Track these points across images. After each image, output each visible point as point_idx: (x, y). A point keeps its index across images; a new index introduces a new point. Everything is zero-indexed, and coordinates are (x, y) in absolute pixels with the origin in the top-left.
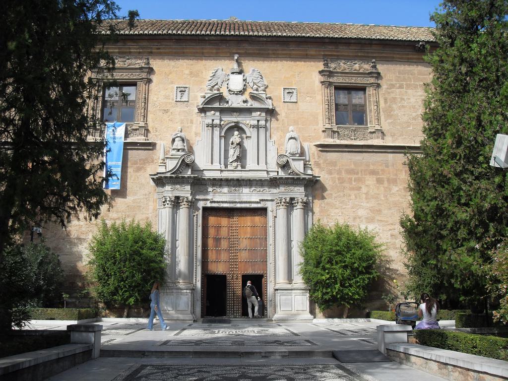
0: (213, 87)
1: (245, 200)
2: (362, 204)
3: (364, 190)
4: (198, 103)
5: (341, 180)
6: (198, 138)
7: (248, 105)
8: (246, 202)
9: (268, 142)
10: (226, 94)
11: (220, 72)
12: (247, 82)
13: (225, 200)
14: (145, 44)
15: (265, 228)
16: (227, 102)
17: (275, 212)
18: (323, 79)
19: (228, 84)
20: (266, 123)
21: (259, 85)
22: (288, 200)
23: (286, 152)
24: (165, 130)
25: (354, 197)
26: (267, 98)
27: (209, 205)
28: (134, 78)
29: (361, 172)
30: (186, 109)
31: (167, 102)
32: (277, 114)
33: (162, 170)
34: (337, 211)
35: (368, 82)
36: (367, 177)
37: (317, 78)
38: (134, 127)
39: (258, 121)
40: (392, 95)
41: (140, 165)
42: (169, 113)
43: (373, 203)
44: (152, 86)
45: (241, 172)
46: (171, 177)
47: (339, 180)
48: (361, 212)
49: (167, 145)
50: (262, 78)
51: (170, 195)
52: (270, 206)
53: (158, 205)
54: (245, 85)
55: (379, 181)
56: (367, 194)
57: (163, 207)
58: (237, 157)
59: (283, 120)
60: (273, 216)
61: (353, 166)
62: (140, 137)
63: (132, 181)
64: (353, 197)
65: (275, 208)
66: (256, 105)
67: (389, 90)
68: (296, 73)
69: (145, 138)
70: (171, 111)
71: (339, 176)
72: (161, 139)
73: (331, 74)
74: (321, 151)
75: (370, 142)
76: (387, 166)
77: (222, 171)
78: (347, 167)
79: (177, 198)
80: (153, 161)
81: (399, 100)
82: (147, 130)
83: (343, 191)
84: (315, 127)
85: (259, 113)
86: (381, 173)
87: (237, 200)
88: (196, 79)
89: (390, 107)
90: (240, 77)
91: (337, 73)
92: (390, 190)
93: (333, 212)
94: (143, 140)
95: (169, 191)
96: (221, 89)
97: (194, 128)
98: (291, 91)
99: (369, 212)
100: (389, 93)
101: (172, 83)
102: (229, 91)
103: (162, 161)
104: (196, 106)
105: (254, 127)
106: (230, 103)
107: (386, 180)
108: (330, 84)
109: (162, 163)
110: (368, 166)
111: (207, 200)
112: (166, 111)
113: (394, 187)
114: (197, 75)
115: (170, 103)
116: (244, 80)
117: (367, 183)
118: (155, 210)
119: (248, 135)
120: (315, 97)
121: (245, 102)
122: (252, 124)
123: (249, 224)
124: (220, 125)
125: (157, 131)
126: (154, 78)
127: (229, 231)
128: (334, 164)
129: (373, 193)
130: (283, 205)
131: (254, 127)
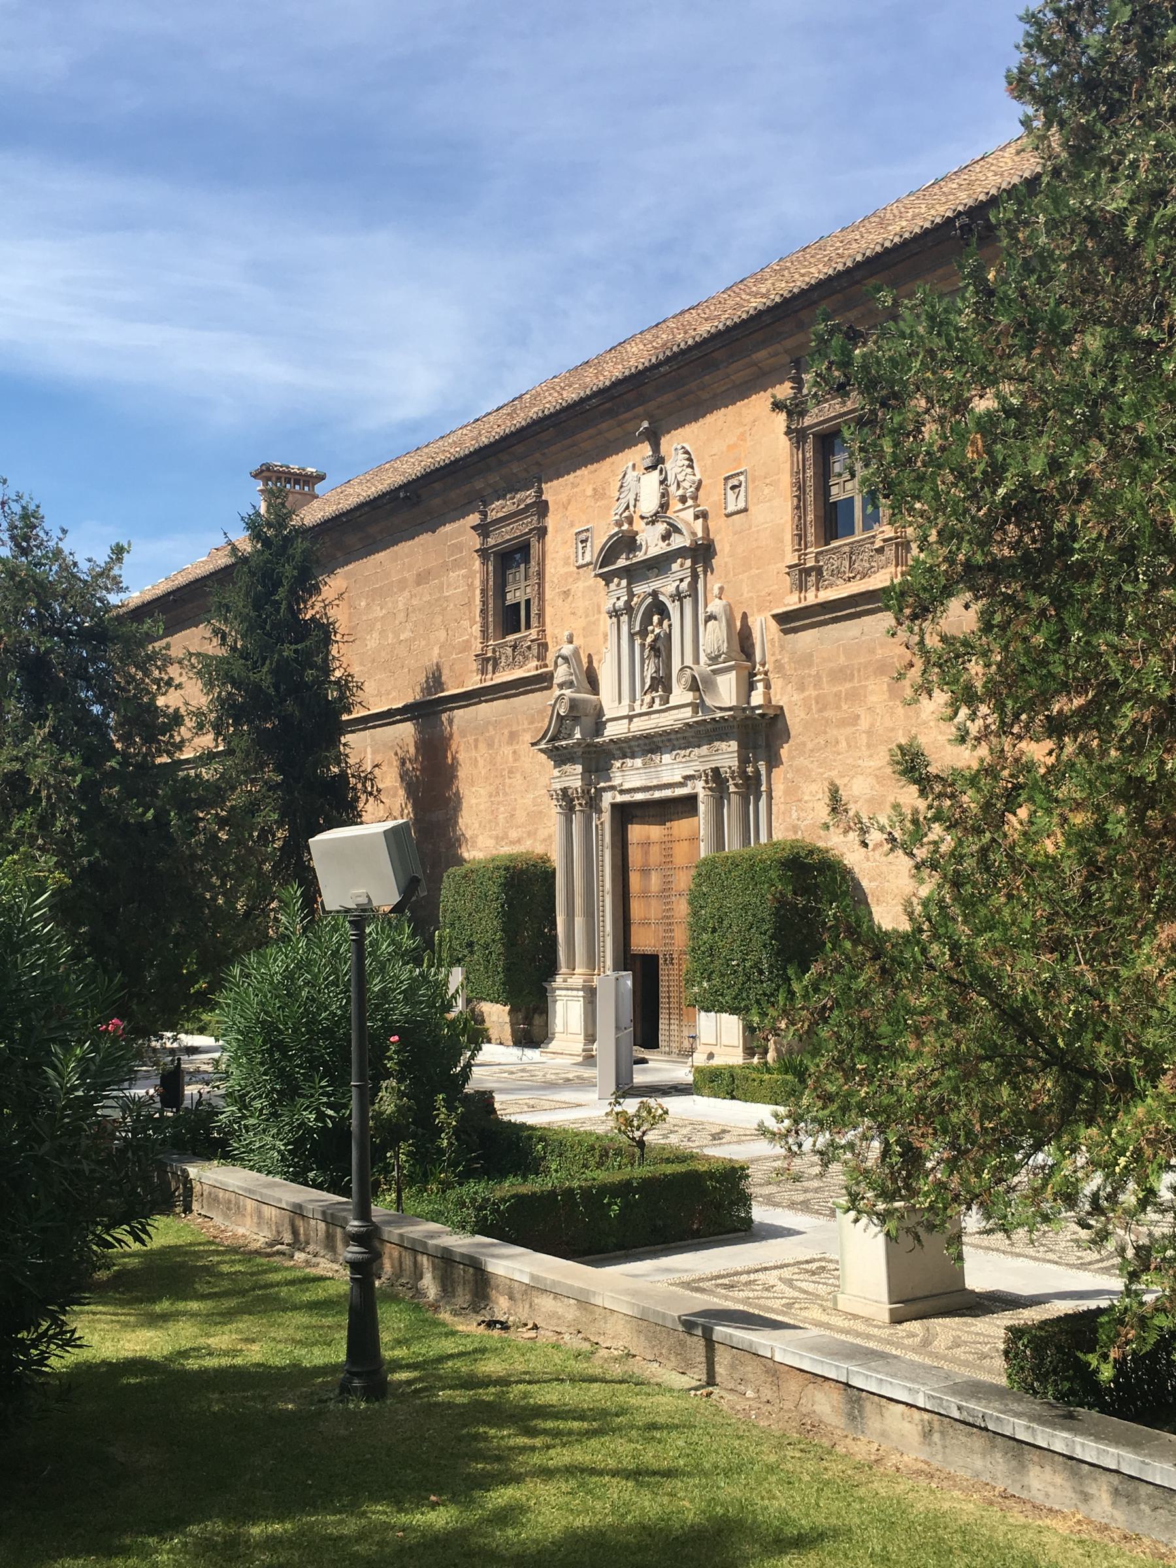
1: (665, 780)
2: (860, 762)
3: (864, 724)
13: (638, 784)
27: (620, 798)
29: (859, 671)
45: (646, 717)
54: (663, 496)
56: (869, 733)
61: (842, 660)
77: (630, 718)
78: (832, 665)
90: (655, 476)
110: (872, 651)
126: (551, 522)
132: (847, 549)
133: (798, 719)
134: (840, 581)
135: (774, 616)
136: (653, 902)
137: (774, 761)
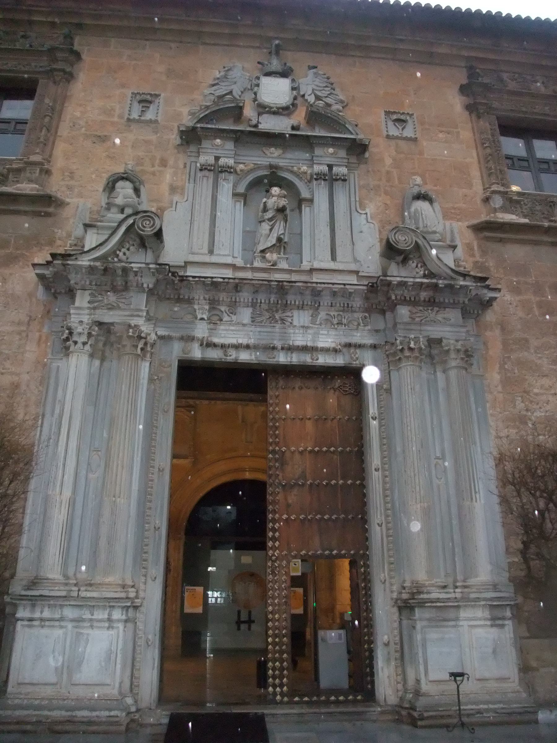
6: (176, 198)
8: (304, 349)
9: (355, 214)
12: (302, 93)
13: (243, 341)
24: (94, 176)
30: (153, 138)
34: (546, 382)
39: (330, 167)
41: (17, 249)
54: (295, 98)
58: (279, 240)
59: (388, 172)
71: (538, 299)
72: (80, 195)
74: (487, 239)
97: (168, 177)
98: (402, 117)
101: (123, 86)
115: (113, 123)
116: (293, 89)
125: (72, 178)
131: (320, 177)
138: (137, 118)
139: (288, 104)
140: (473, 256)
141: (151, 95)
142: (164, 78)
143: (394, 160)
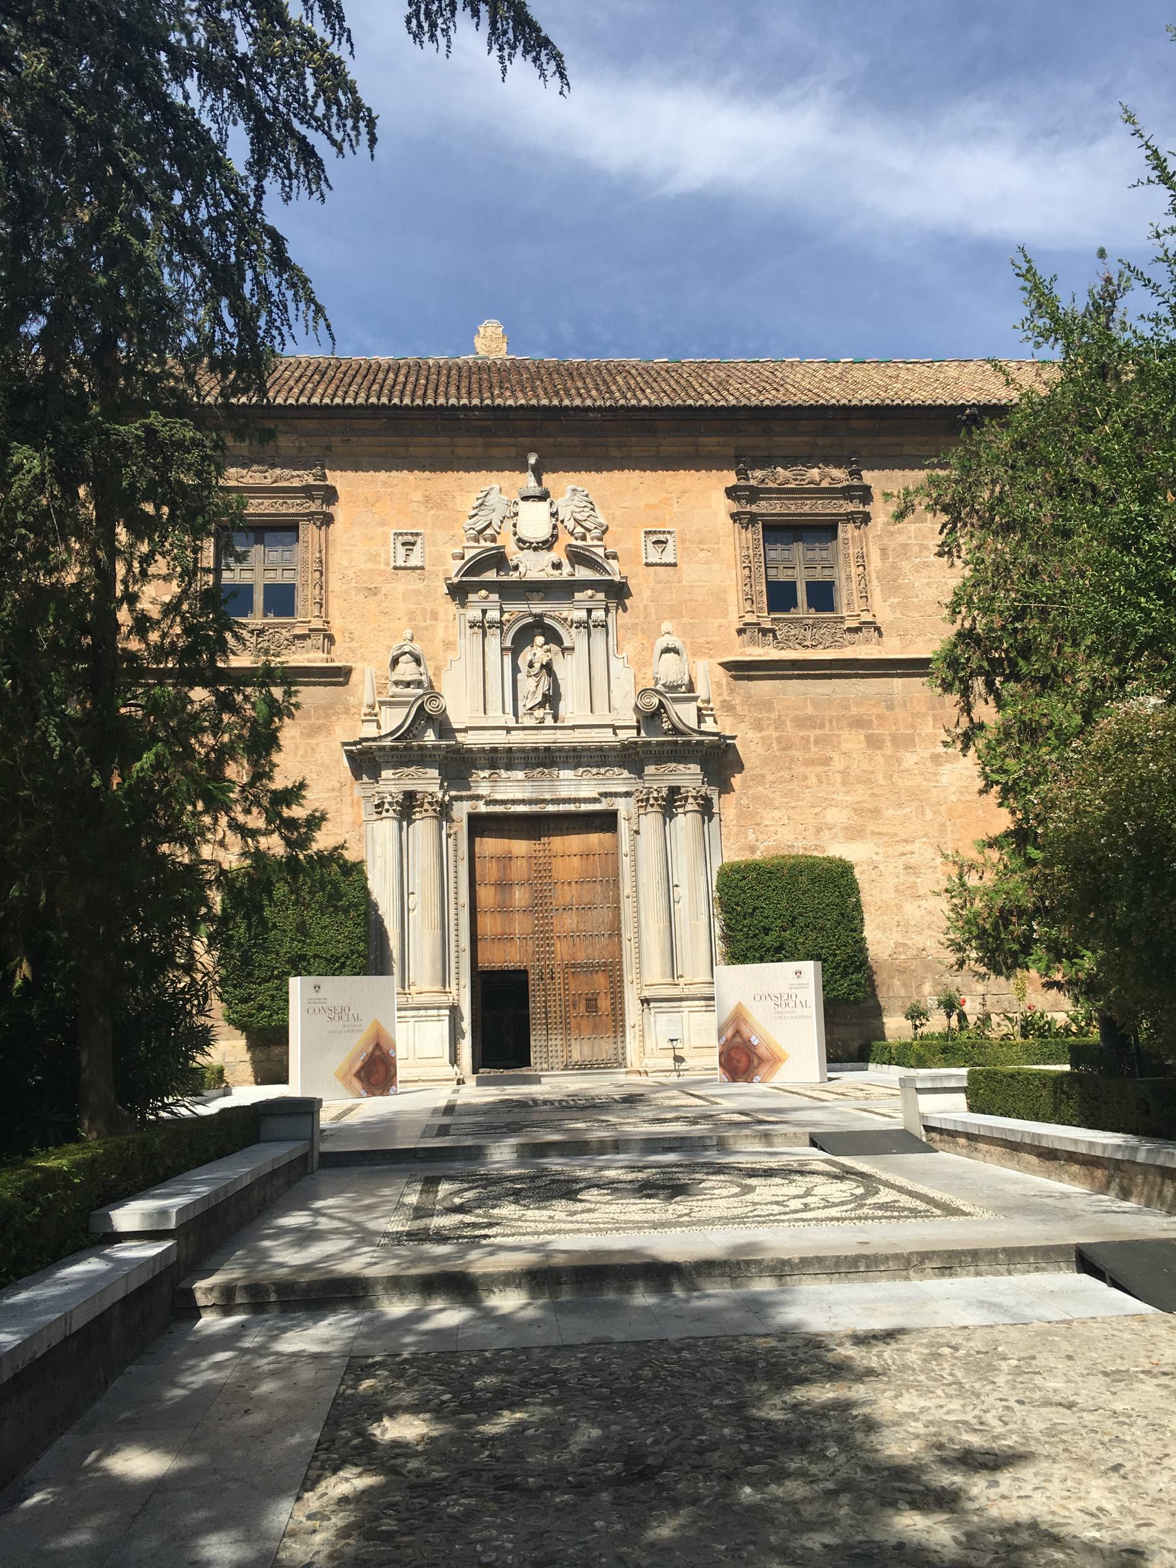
0: (481, 532)
1: (564, 794)
2: (835, 796)
3: (838, 764)
4: (446, 571)
5: (786, 745)
7: (565, 573)
9: (612, 658)
10: (511, 549)
11: (493, 499)
12: (560, 518)
13: (519, 796)
14: (312, 425)
15: (613, 854)
16: (516, 568)
17: (634, 820)
18: (735, 507)
19: (515, 525)
20: (607, 616)
21: (587, 524)
22: (664, 792)
23: (656, 683)
25: (814, 780)
26: (607, 557)
27: (483, 808)
28: (292, 511)
29: (831, 722)
30: (420, 586)
31: (374, 571)
32: (629, 594)
33: (370, 731)
34: (776, 814)
35: (842, 511)
36: (845, 734)
37: (723, 506)
38: (297, 631)
39: (589, 611)
40: (900, 539)
42: (380, 597)
43: (859, 794)
44: (336, 528)
46: (393, 748)
47: (779, 742)
48: (833, 816)
49: (380, 673)
50: (593, 510)
51: (393, 789)
52: (622, 806)
53: (363, 813)
54: (555, 527)
55: (873, 742)
56: (845, 773)
57: (375, 816)
58: (544, 695)
60: (630, 830)
61: (810, 710)
62: (312, 655)
63: (298, 758)
64: (813, 780)
65: (633, 810)
66: (583, 573)
67: (891, 528)
68: (673, 495)
69: (325, 655)
70: (383, 591)
71: (778, 734)
73: (754, 495)
74: (736, 678)
75: (848, 653)
76: (890, 707)
79: (410, 796)
80: (347, 711)
81: (916, 549)
82: (331, 639)
83: (790, 769)
84: (720, 620)
85: (590, 592)
86: (875, 722)
87: (548, 796)
88: (439, 512)
89: (894, 566)
90: (544, 507)
91: (769, 490)
92: (899, 761)
93: (768, 816)
94: (322, 661)
95: (392, 783)
96: (498, 537)
97: (440, 632)
98: (662, 537)
99: (852, 813)
100: (892, 534)
101: (383, 523)
102: (520, 540)
103: (368, 711)
104: (442, 577)
105: (580, 624)
106: (522, 569)
107: (888, 738)
108: (753, 518)
109: (370, 714)
110: (847, 707)
111: (478, 797)
112: (373, 592)
113: (908, 754)
114: (441, 506)
115: (381, 573)
117: (845, 747)
118: (358, 824)
119: (567, 644)
120: (719, 549)
121: (557, 566)
122: (576, 619)
123: (575, 850)
124: (501, 622)
125: (352, 639)
126: (339, 511)
127: (530, 868)
128: (766, 705)
129: (858, 772)
130: (652, 806)
131: (580, 624)
132: (811, 622)
133: (754, 755)
134: (797, 646)
135: (722, 664)
136: (517, 917)
137: (725, 788)
138: (403, 565)
139: (548, 536)
140: (720, 695)
141: (412, 534)
142: (422, 509)
143: (653, 591)
